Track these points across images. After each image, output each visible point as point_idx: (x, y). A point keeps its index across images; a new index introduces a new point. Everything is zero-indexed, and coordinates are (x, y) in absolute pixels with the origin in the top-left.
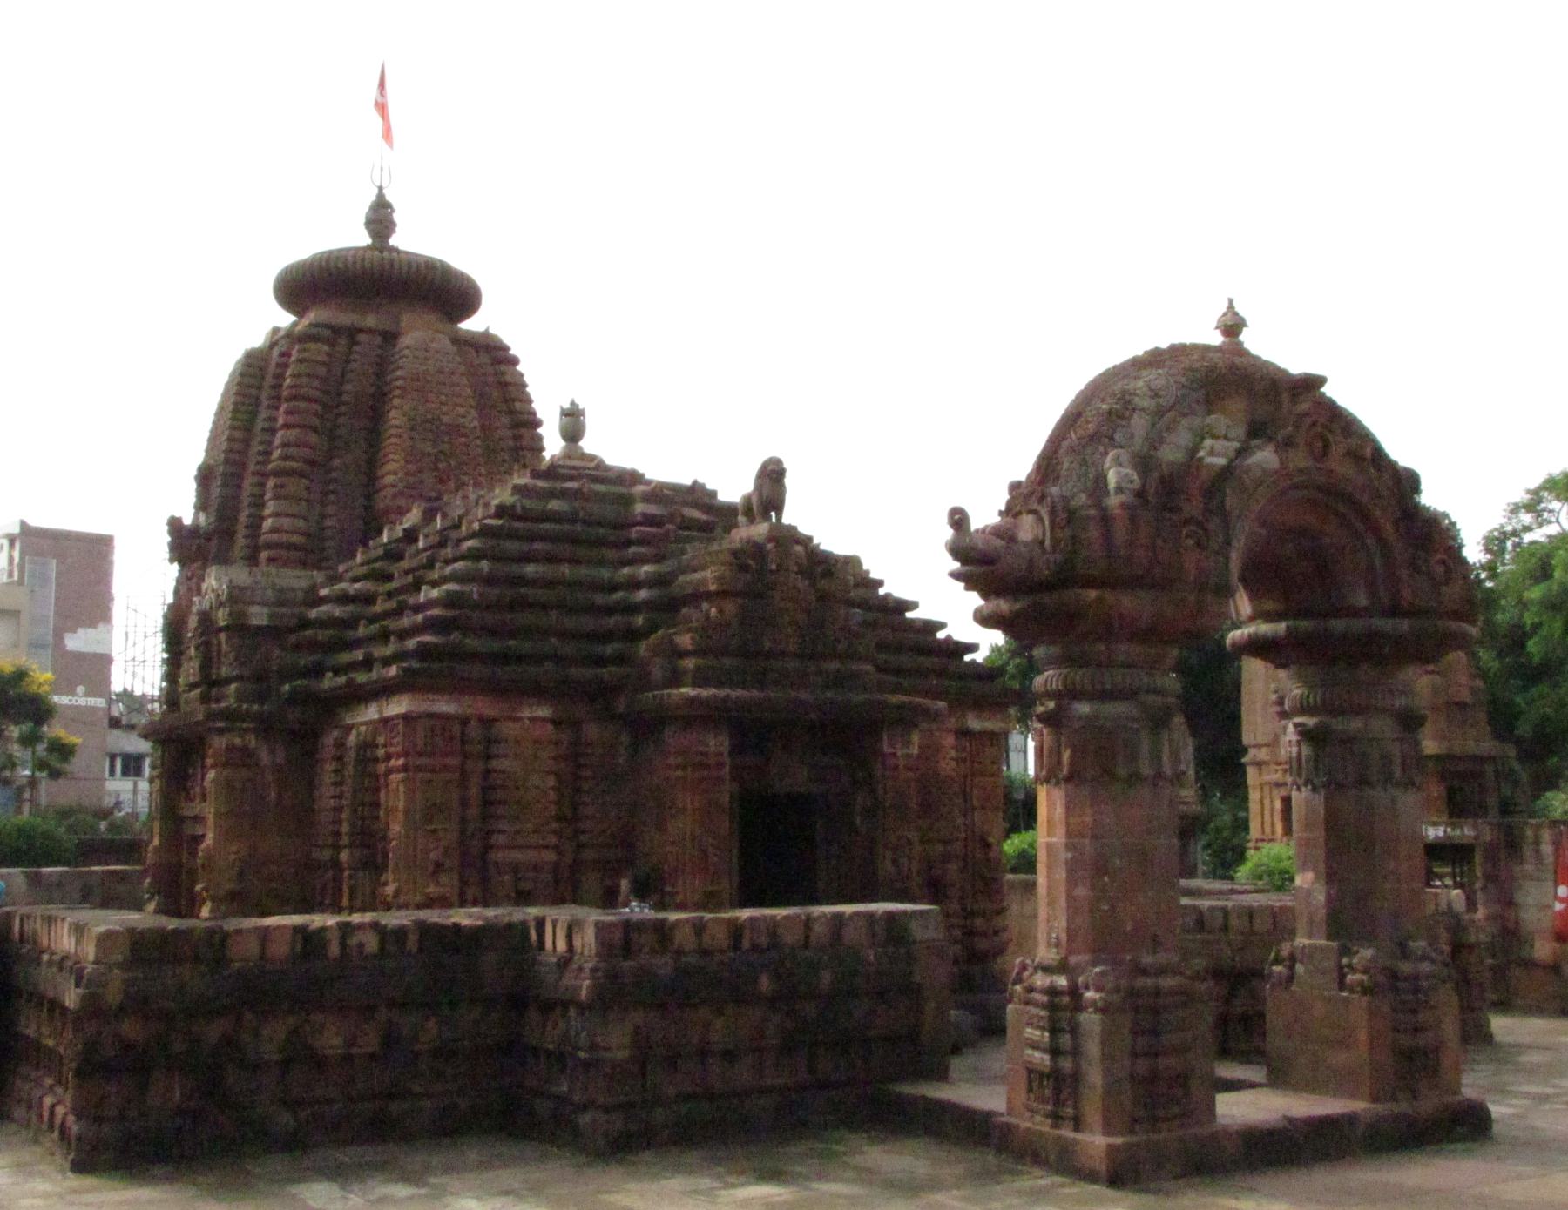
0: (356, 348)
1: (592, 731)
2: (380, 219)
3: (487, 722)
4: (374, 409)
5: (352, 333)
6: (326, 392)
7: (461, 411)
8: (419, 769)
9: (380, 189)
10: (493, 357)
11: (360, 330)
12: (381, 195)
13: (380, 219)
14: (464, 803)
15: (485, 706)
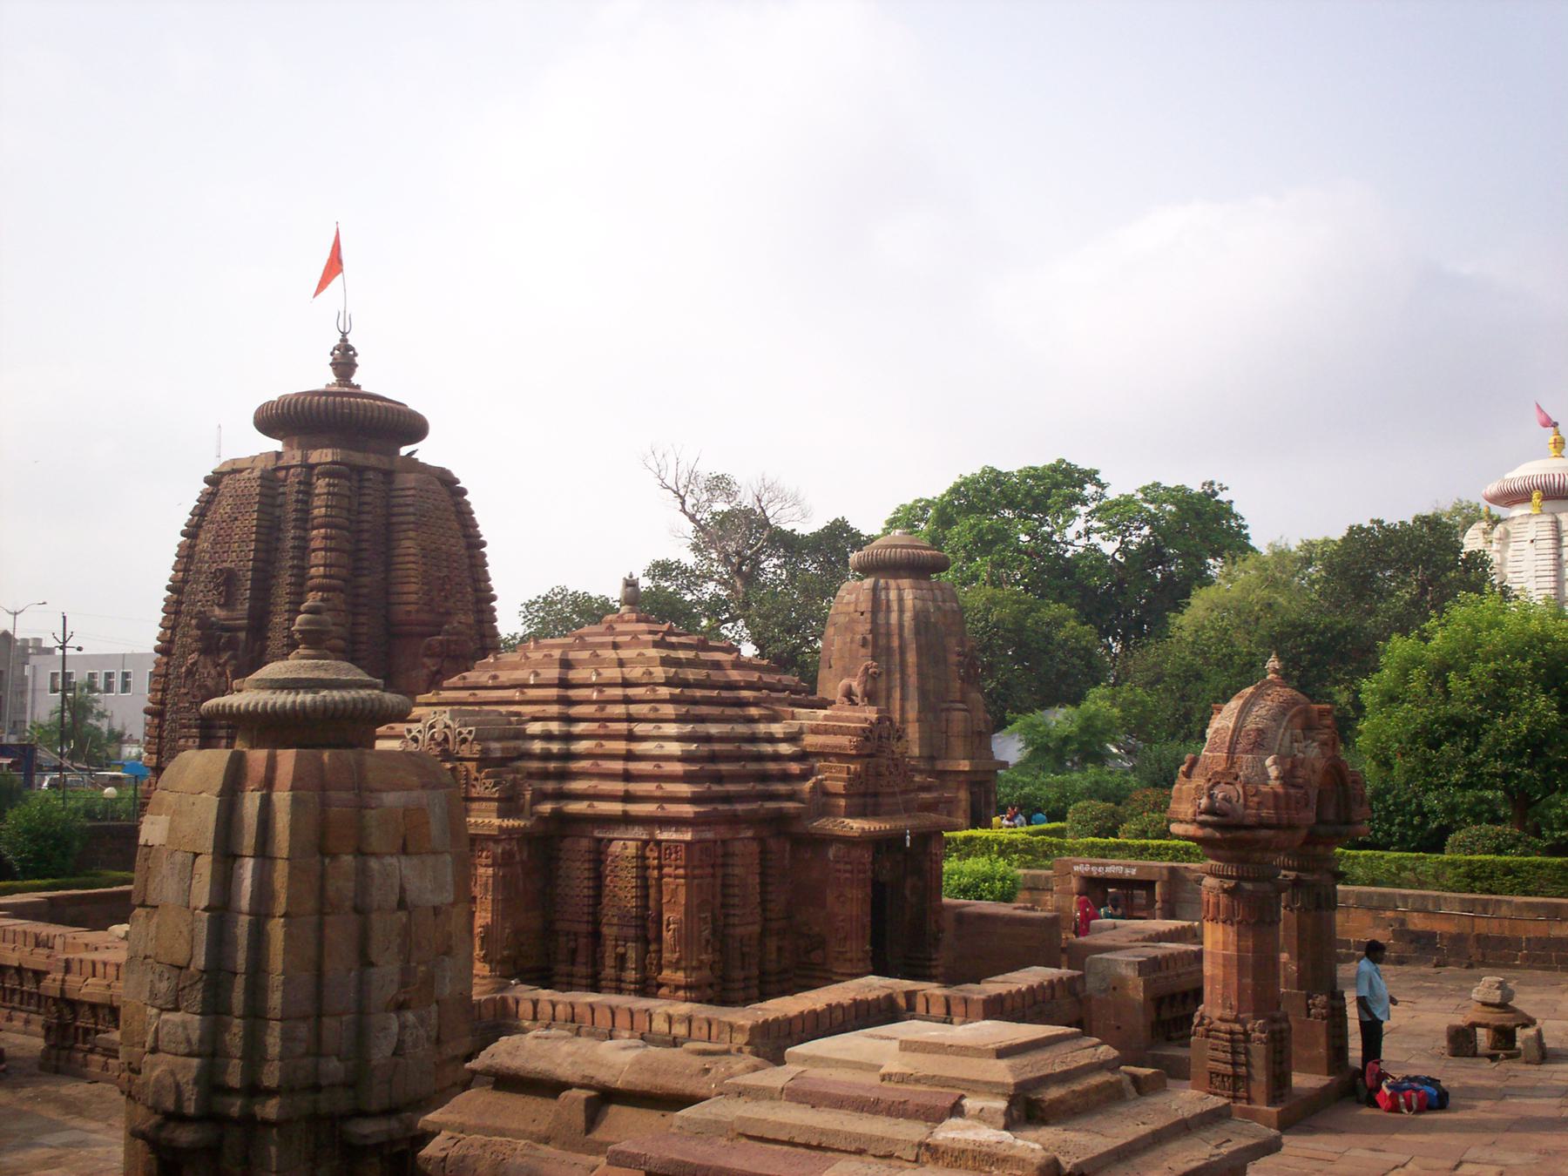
0: (367, 484)
1: (773, 844)
2: (344, 361)
3: (724, 842)
4: (388, 535)
5: (360, 470)
6: (351, 522)
7: (452, 541)
8: (694, 877)
9: (344, 334)
10: (446, 485)
11: (367, 468)
12: (344, 340)
13: (344, 361)
14: (714, 897)
15: (724, 832)
